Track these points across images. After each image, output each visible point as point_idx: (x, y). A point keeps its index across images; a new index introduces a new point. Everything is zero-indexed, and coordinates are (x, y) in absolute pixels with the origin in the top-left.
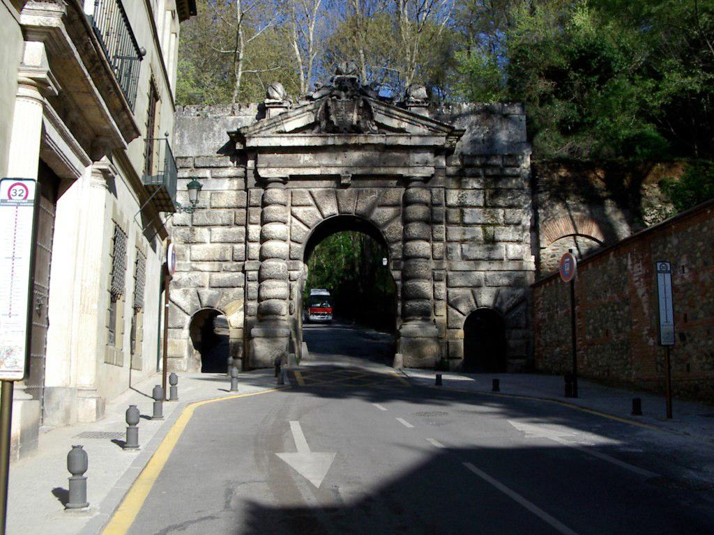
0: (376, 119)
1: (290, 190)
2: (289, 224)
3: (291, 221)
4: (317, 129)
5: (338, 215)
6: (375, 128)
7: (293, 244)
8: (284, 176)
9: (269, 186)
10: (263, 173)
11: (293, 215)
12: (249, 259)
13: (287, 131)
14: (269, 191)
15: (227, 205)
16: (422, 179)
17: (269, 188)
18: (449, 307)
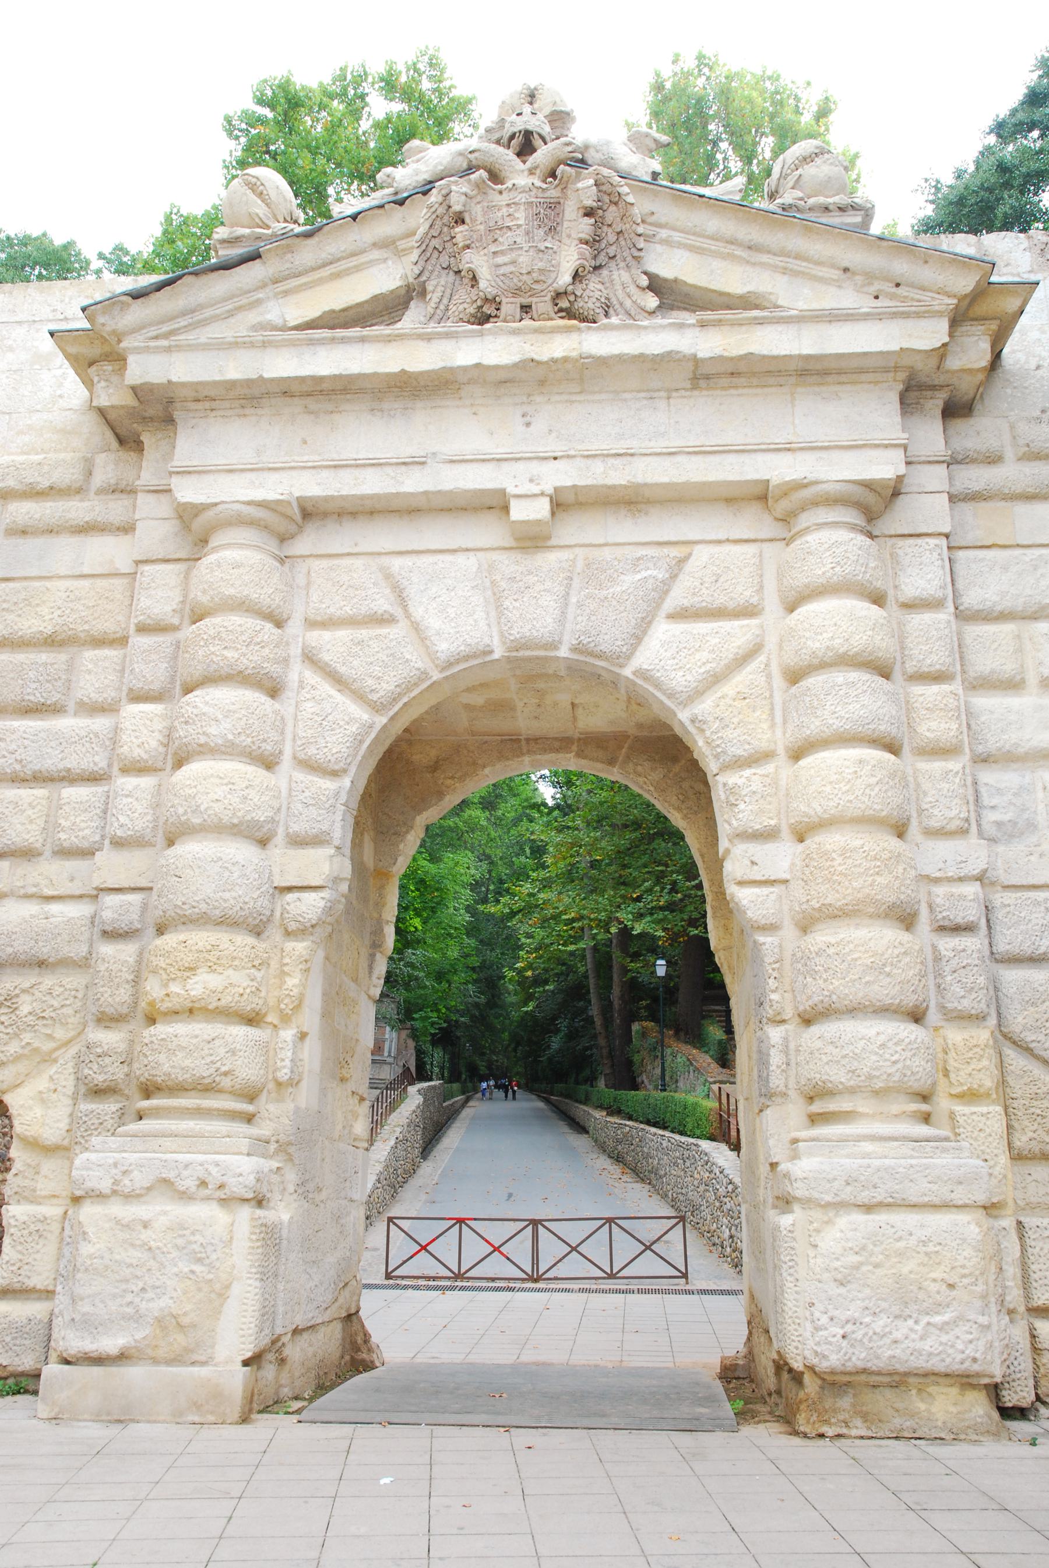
0: (653, 269)
1: (302, 567)
2: (289, 695)
3: (301, 685)
4: (412, 318)
5: (496, 655)
6: (652, 301)
7: (301, 777)
8: (272, 496)
9: (211, 545)
10: (188, 492)
11: (310, 658)
12: (118, 843)
13: (292, 324)
14: (212, 558)
15: (49, 630)
16: (859, 491)
17: (215, 549)
18: (1010, 1052)
